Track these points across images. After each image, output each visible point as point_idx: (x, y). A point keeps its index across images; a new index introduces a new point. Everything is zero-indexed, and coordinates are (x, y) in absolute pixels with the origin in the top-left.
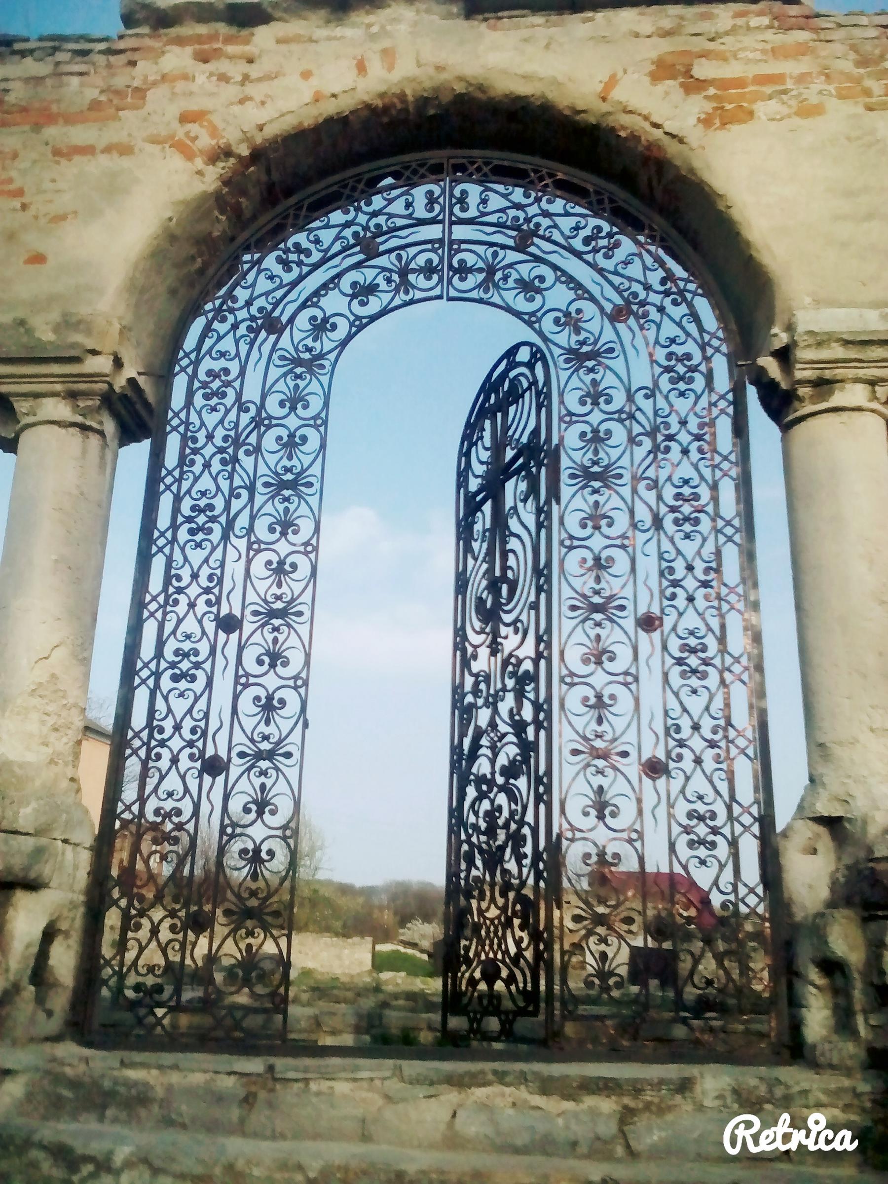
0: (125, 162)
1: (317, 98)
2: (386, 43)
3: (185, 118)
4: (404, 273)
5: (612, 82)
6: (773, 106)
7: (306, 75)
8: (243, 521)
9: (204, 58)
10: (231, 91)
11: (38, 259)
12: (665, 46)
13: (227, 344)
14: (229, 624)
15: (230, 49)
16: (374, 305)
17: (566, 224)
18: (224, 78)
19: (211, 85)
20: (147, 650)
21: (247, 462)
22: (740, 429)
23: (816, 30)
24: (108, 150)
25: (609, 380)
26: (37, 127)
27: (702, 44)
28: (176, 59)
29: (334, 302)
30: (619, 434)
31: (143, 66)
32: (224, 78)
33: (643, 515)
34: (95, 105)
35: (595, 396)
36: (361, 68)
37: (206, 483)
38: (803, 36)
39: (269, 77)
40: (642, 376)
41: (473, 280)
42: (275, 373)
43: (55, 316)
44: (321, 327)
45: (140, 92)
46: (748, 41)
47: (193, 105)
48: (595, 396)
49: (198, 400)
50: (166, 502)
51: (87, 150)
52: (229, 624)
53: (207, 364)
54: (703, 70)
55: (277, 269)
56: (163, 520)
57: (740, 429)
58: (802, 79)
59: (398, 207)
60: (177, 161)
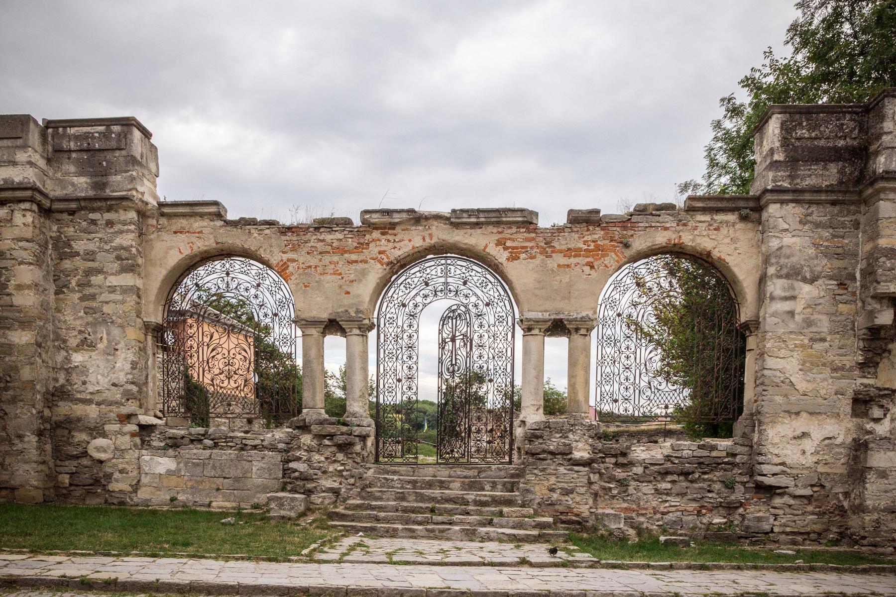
0: (366, 266)
1: (413, 248)
2: (430, 232)
3: (380, 253)
4: (435, 291)
5: (486, 246)
6: (523, 256)
7: (410, 241)
8: (400, 356)
9: (383, 234)
10: (391, 245)
11: (348, 293)
12: (500, 236)
13: (393, 310)
14: (399, 380)
15: (390, 231)
16: (429, 300)
17: (475, 279)
18: (389, 241)
19: (386, 243)
20: (381, 386)
21: (400, 341)
22: (513, 336)
23: (536, 233)
24: (361, 262)
25: (485, 322)
26: (342, 254)
27: (509, 236)
28: (376, 234)
29: (419, 299)
30: (486, 336)
31: (368, 236)
32: (389, 241)
33: (491, 356)
34: (356, 248)
35: (481, 326)
36: (424, 239)
37: (391, 346)
38: (533, 235)
39: (400, 241)
40: (492, 322)
41: (453, 294)
42: (405, 318)
43: (354, 309)
44: (416, 306)
45: (368, 244)
46: (520, 236)
47: (382, 249)
48: (481, 326)
49: (387, 325)
50: (382, 351)
51: (356, 262)
52: (399, 380)
53: (388, 315)
54: (509, 244)
55: (404, 289)
56: (382, 356)
57: (513, 336)
58: (532, 248)
59: (433, 272)
60: (379, 266)
